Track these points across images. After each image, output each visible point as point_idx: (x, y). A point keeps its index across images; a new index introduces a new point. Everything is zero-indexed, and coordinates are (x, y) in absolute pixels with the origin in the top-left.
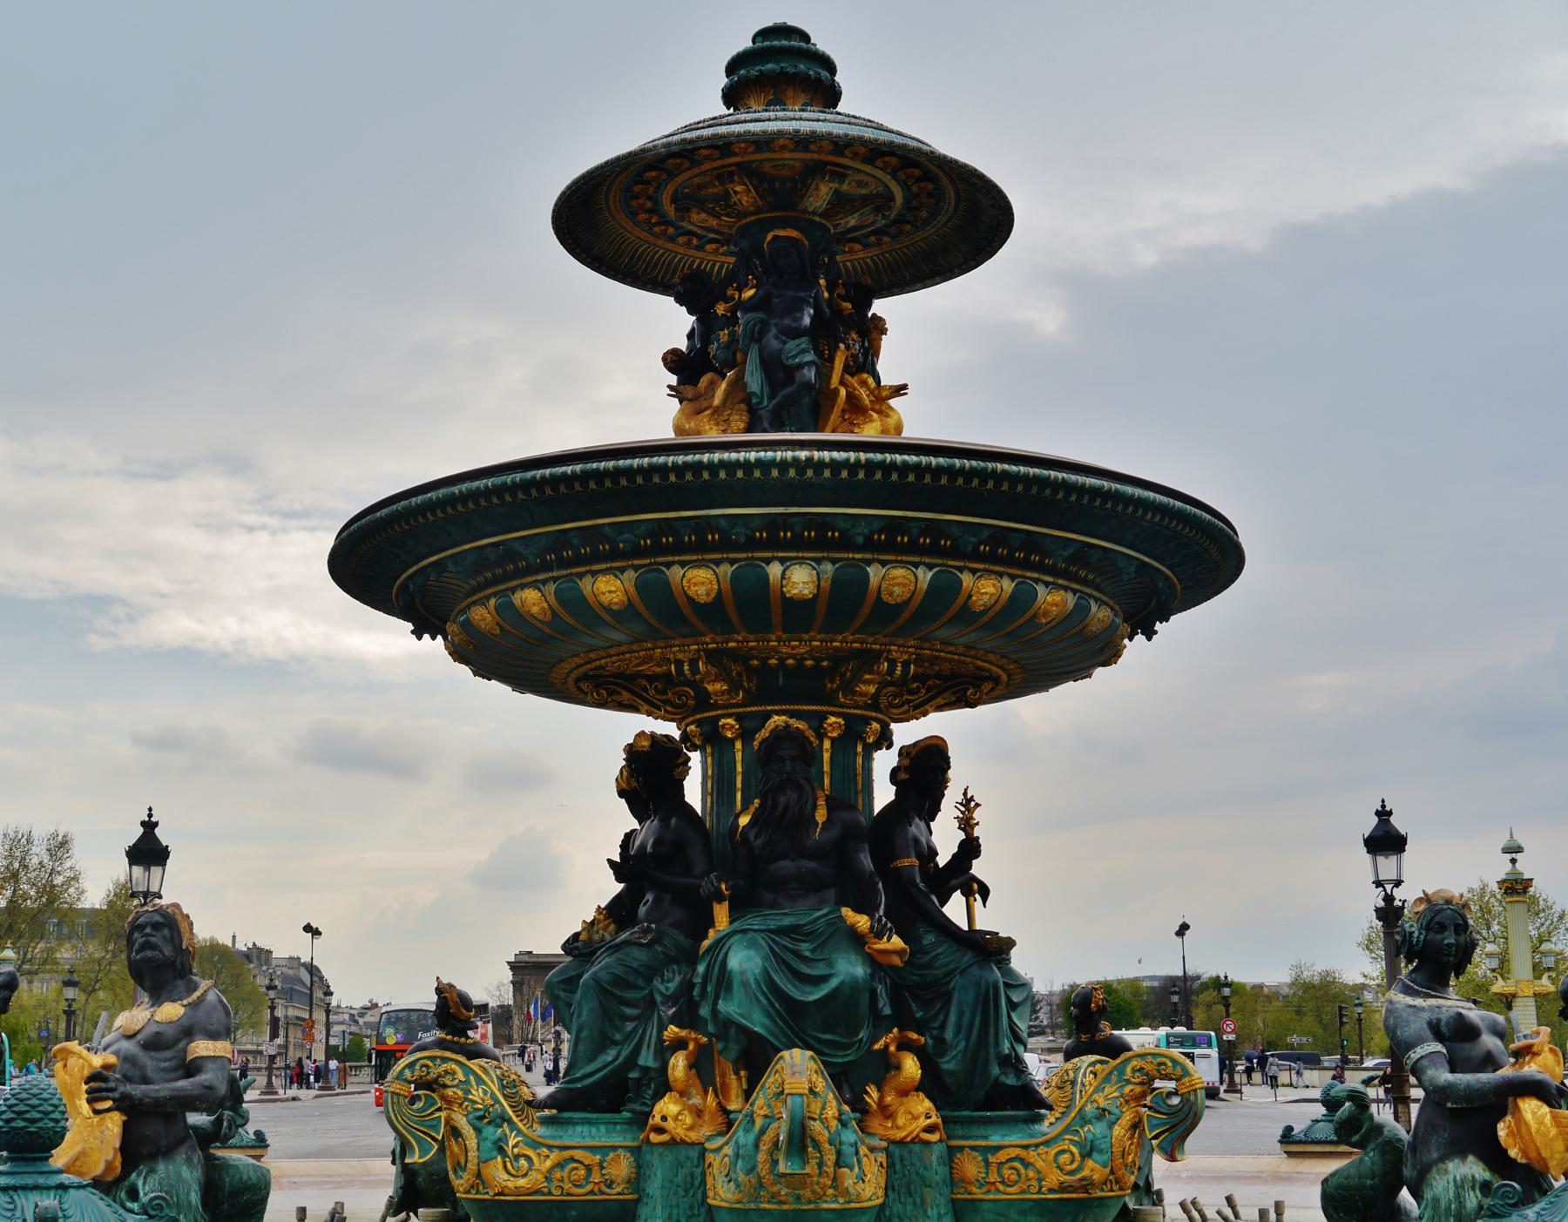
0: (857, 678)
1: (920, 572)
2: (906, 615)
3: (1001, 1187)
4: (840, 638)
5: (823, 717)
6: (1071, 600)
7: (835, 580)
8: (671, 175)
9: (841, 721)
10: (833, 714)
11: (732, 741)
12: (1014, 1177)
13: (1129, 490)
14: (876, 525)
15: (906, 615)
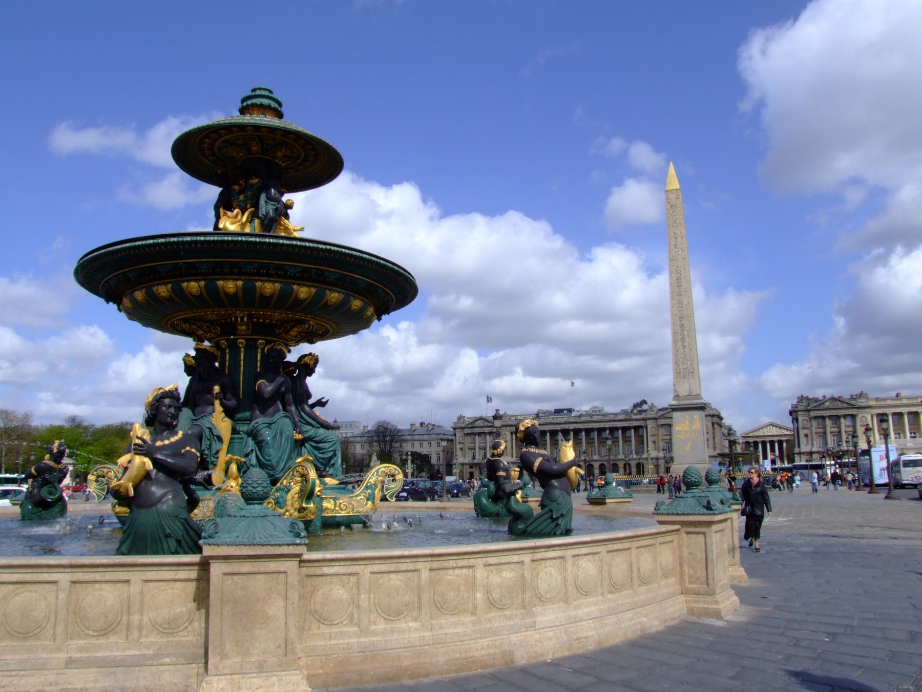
0: (291, 328)
1: (277, 285)
2: (274, 301)
3: (340, 511)
4: (278, 312)
5: (258, 340)
6: (342, 296)
7: (281, 290)
8: (221, 136)
9: (263, 341)
10: (261, 339)
11: (225, 350)
12: (345, 508)
13: (354, 253)
14: (299, 269)
15: (274, 301)
